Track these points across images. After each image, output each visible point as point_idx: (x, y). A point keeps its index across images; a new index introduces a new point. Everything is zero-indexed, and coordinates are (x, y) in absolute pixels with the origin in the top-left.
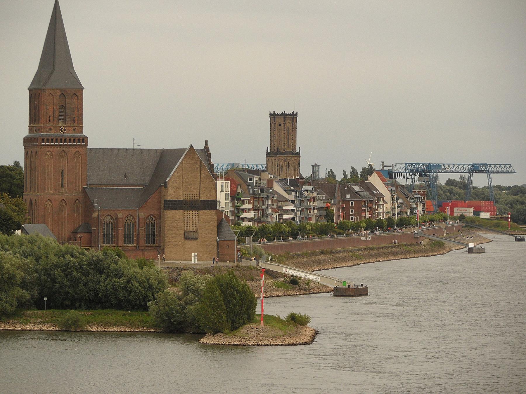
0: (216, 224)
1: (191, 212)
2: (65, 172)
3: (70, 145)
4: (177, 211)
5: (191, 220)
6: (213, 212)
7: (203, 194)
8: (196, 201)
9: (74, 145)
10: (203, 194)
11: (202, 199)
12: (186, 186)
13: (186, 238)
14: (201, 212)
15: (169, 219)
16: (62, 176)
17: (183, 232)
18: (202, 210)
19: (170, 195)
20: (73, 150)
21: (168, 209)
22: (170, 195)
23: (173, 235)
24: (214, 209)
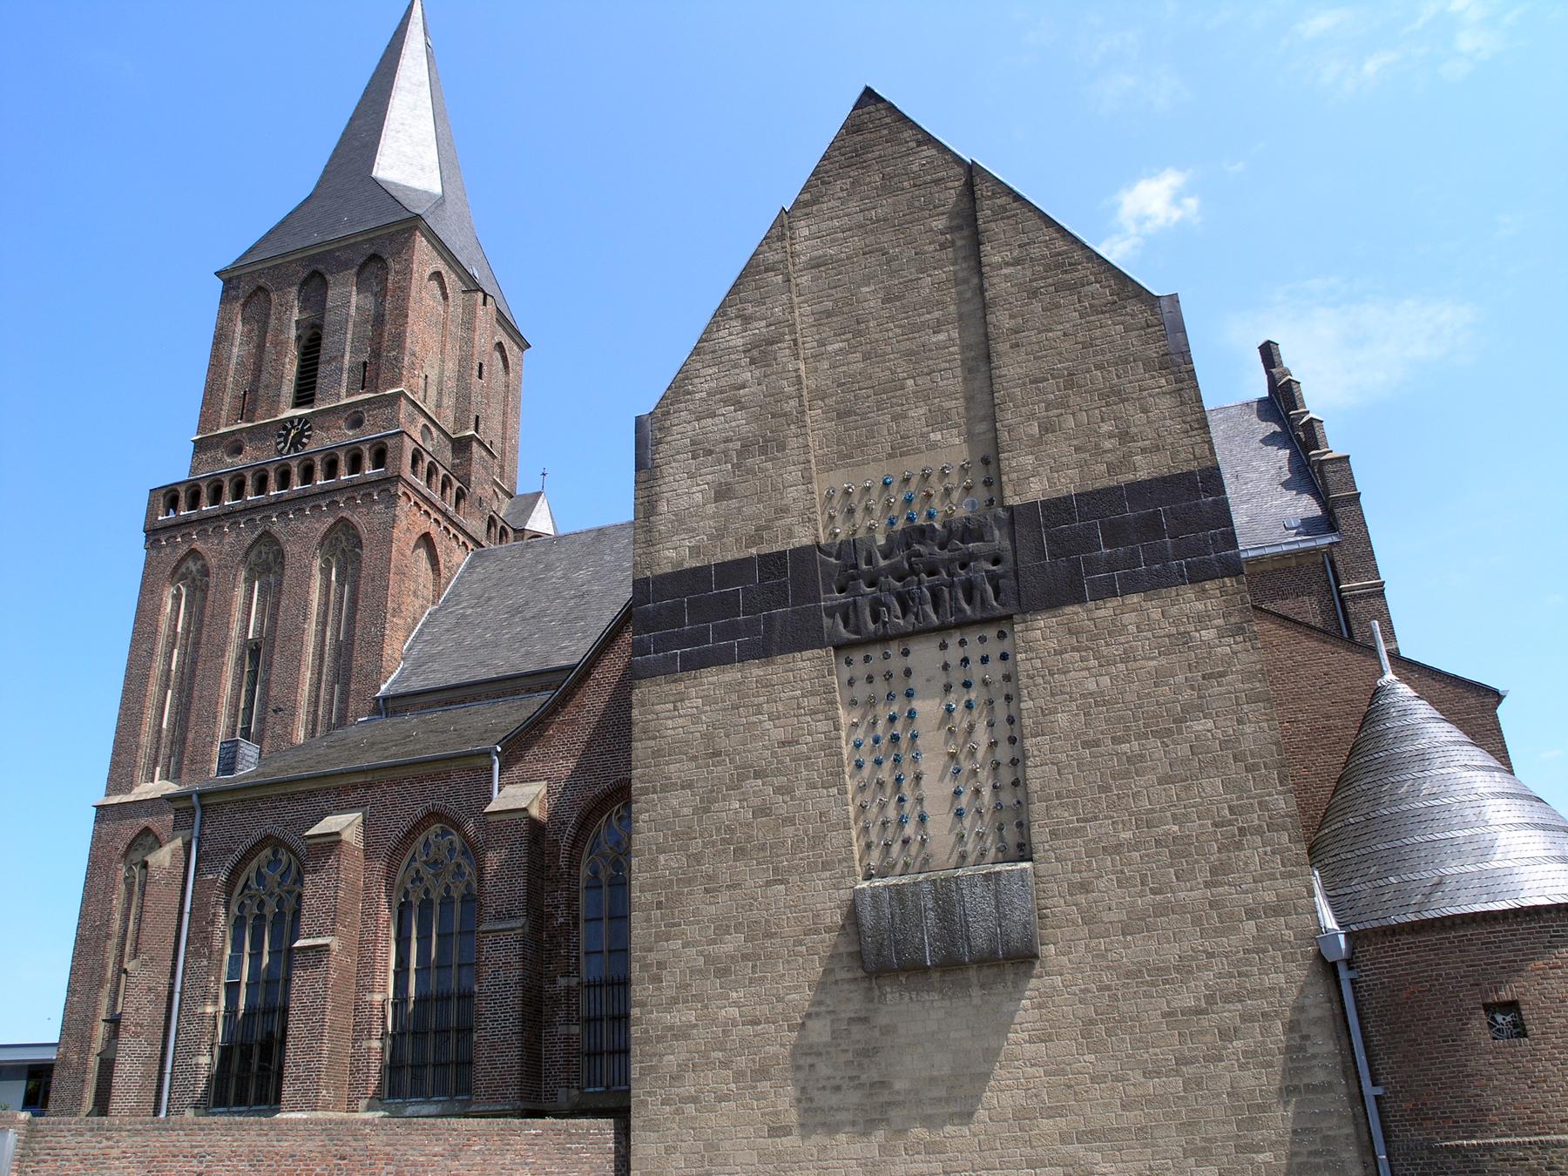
11: (1036, 490)
18: (1053, 600)
21: (666, 669)
23: (732, 944)
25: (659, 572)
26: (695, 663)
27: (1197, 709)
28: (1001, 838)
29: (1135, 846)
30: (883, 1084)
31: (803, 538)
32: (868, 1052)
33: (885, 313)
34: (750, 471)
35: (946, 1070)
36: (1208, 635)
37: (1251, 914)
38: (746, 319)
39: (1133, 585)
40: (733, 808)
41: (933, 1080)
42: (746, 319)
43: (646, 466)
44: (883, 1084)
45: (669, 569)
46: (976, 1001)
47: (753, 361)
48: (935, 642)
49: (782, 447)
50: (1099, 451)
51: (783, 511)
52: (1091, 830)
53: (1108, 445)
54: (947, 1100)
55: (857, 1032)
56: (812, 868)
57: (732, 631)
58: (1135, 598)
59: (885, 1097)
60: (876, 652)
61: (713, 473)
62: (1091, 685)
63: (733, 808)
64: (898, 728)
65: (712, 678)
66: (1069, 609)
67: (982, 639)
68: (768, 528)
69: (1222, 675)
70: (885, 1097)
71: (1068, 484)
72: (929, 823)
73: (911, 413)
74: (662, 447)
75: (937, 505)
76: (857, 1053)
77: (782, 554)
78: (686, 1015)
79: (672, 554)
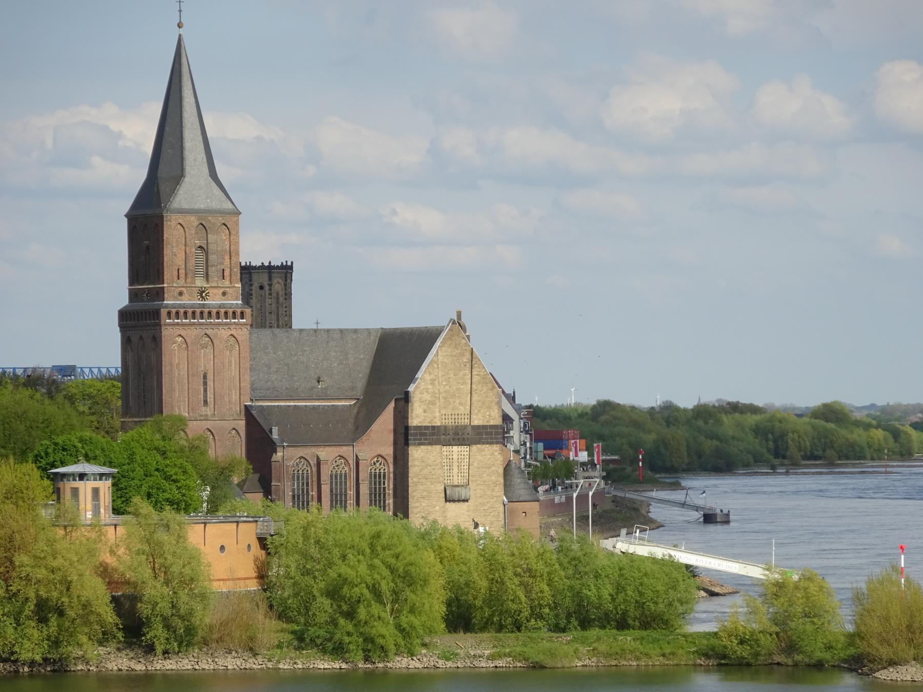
0: (501, 471)
2: (210, 377)
3: (219, 324)
4: (429, 447)
5: (455, 464)
7: (477, 414)
8: (465, 427)
9: (226, 324)
10: (477, 414)
11: (476, 422)
13: (447, 500)
15: (416, 463)
16: (205, 384)
17: (443, 488)
18: (476, 444)
19: (417, 416)
20: (224, 333)
22: (417, 416)
23: (425, 494)
31: (439, 424)
39: (488, 443)
40: (425, 472)
57: (426, 439)
63: (425, 472)
65: (422, 447)
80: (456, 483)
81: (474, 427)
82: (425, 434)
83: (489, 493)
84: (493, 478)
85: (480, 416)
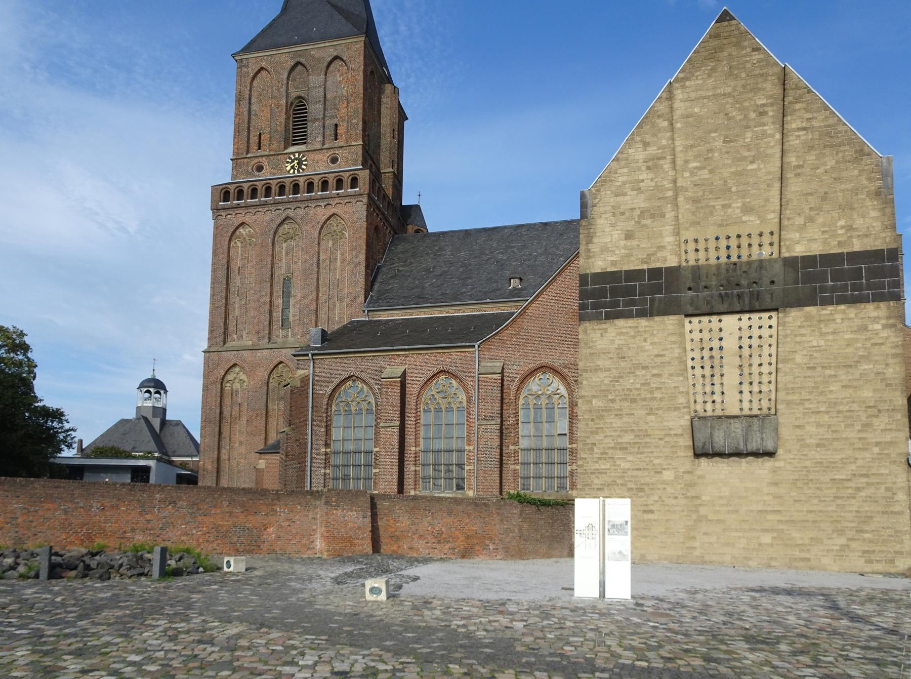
1: (730, 321)
6: (874, 313)
7: (802, 228)
10: (802, 228)
11: (799, 250)
12: (695, 201)
14: (795, 316)
19: (605, 249)
21: (597, 318)
22: (605, 249)
24: (878, 298)
25: (593, 271)
26: (610, 317)
27: (867, 358)
28: (760, 404)
29: (827, 412)
30: (698, 497)
31: (672, 262)
32: (692, 485)
33: (724, 150)
34: (645, 226)
35: (727, 494)
36: (878, 327)
37: (877, 444)
38: (646, 144)
41: (721, 498)
42: (646, 144)
43: (586, 217)
44: (698, 497)
45: (599, 271)
46: (743, 468)
47: (648, 168)
48: (737, 316)
49: (664, 217)
50: (834, 235)
51: (661, 248)
52: (807, 405)
53: (840, 232)
54: (727, 505)
55: (687, 477)
56: (669, 409)
57: (633, 303)
58: (842, 307)
59: (699, 502)
60: (705, 319)
61: (625, 225)
62: (815, 344)
64: (714, 353)
66: (808, 309)
67: (760, 318)
68: (653, 255)
69: (882, 344)
70: (699, 502)
71: (816, 249)
72: (726, 395)
73: (734, 205)
74: (595, 209)
75: (745, 253)
76: (686, 485)
77: (661, 269)
78: (603, 466)
79: (600, 263)
80: (733, 409)
81: (791, 263)
82: (630, 291)
83: (852, 434)
84: (867, 394)
85: (814, 231)
